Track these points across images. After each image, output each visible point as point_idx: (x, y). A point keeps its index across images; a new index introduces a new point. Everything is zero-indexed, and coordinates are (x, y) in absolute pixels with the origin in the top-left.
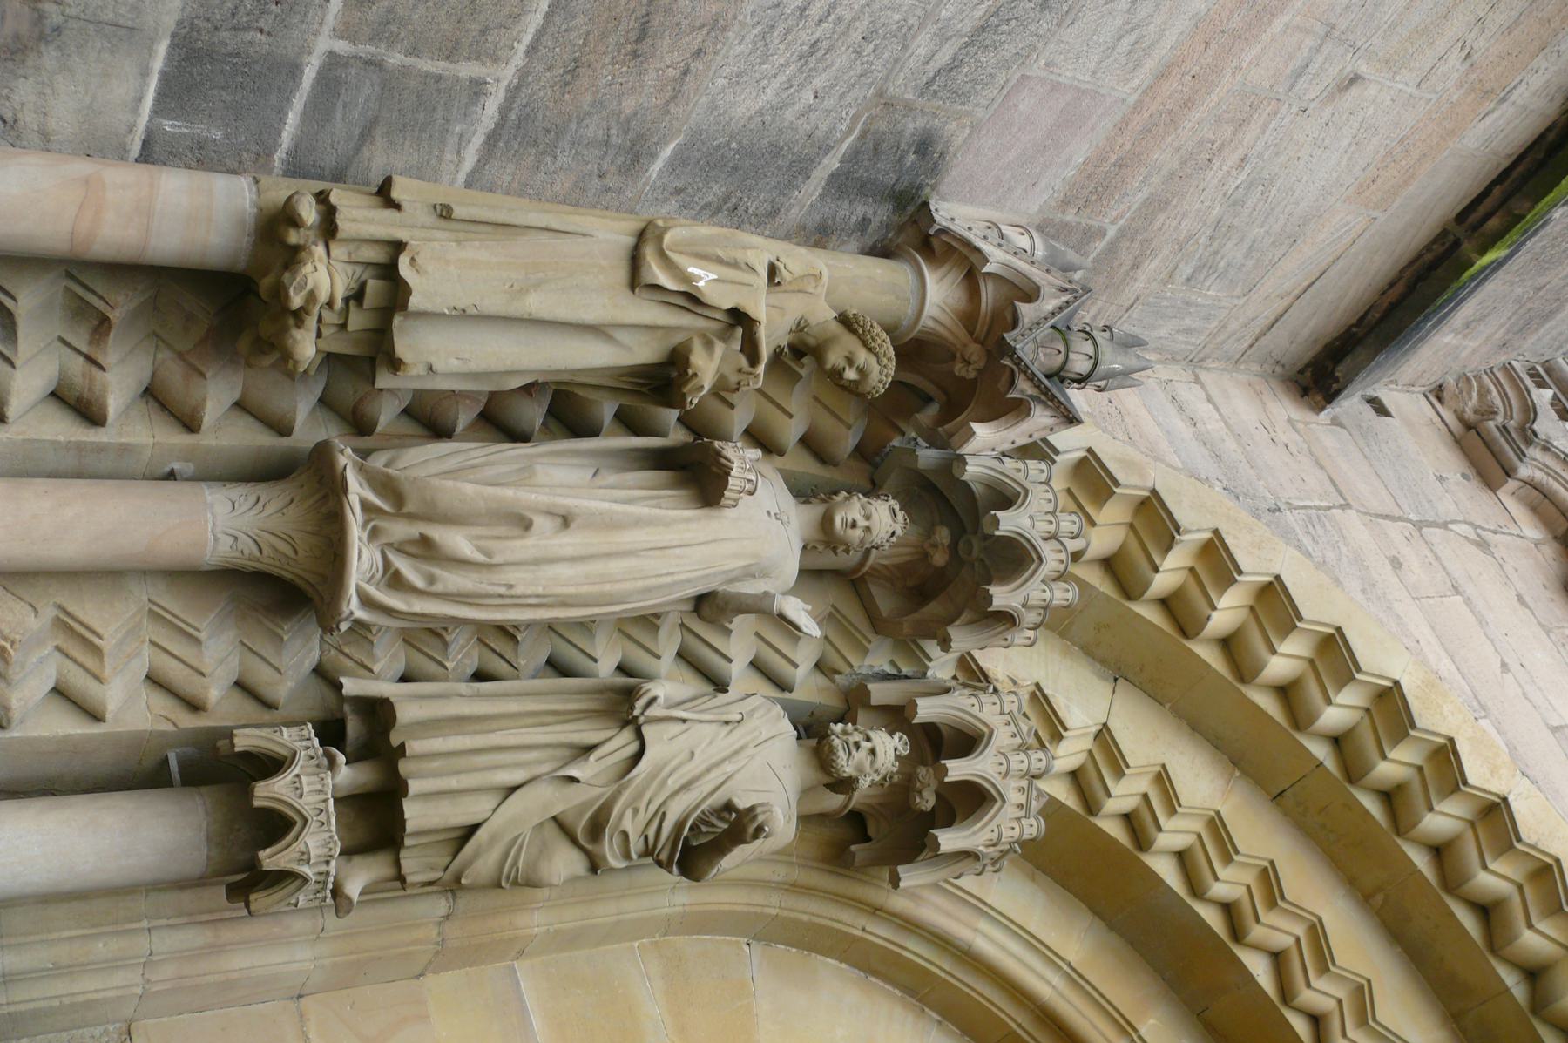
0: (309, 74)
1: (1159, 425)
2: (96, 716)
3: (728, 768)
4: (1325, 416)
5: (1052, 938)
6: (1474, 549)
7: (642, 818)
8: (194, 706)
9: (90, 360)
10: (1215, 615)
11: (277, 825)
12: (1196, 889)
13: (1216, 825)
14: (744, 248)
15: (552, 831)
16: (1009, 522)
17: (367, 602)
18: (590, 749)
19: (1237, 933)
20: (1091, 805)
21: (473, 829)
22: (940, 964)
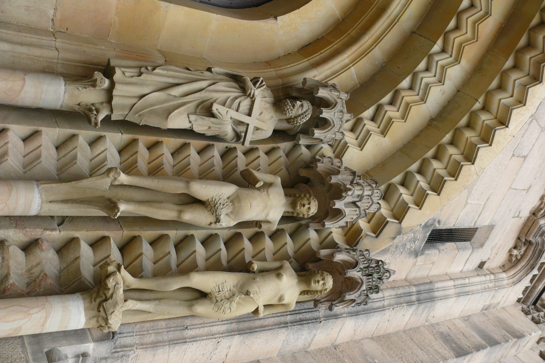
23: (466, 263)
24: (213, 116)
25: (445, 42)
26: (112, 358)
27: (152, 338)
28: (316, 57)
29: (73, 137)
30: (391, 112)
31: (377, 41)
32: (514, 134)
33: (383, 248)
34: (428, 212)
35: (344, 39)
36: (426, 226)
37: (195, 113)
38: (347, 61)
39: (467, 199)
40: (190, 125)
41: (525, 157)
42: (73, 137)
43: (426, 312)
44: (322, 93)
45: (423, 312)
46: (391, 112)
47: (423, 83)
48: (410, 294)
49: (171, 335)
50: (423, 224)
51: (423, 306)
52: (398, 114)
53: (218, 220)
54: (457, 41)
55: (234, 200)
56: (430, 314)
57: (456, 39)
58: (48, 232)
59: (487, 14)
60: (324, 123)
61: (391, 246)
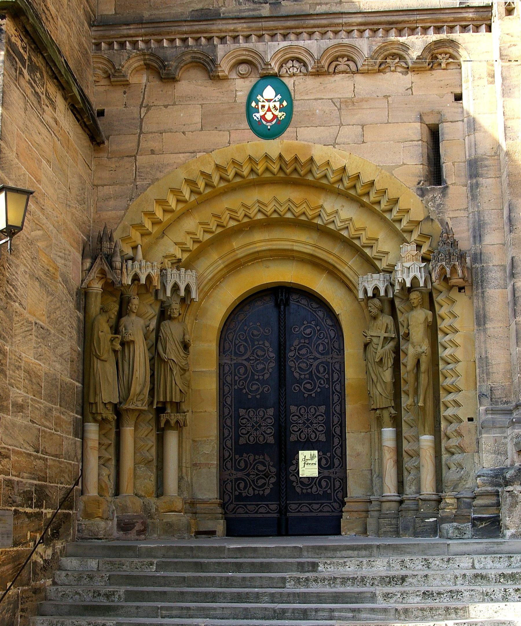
0: (76, 415)
1: (111, 210)
2: (153, 446)
3: (176, 343)
4: (106, 142)
5: (212, 260)
6: (150, 111)
7: (183, 361)
8: (152, 430)
9: (103, 445)
10: (160, 218)
11: (177, 422)
12: (212, 232)
13: (201, 223)
14: (99, 337)
15: (182, 376)
16: (143, 281)
17: (145, 405)
18: (170, 368)
19: (223, 227)
20: (190, 251)
21: (180, 390)
22: (211, 284)
23: (455, 122)
24: (382, 359)
25: (314, 218)
26: (491, 395)
27: (485, 375)
28: (351, 286)
29: (405, 421)
30: (364, 240)
31: (330, 253)
32: (348, 154)
33: (440, 226)
34: (412, 200)
35: (336, 272)
36: (422, 193)
37: (382, 367)
38: (346, 268)
39: (400, 166)
40: (389, 369)
41: (363, 126)
42: (405, 421)
43: (486, 163)
44: (361, 296)
45: (486, 166)
46: (364, 240)
47: (341, 224)
48: (471, 187)
49: (484, 365)
50: (421, 199)
51: (480, 171)
52: (363, 233)
53: (423, 352)
54: (311, 213)
55: (414, 347)
56: (489, 156)
57: (310, 213)
58: (442, 429)
59: (289, 200)
60: (376, 289)
61: (438, 219)
